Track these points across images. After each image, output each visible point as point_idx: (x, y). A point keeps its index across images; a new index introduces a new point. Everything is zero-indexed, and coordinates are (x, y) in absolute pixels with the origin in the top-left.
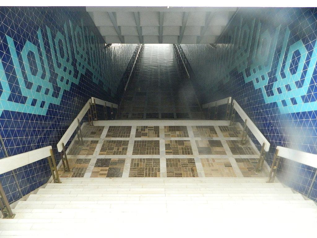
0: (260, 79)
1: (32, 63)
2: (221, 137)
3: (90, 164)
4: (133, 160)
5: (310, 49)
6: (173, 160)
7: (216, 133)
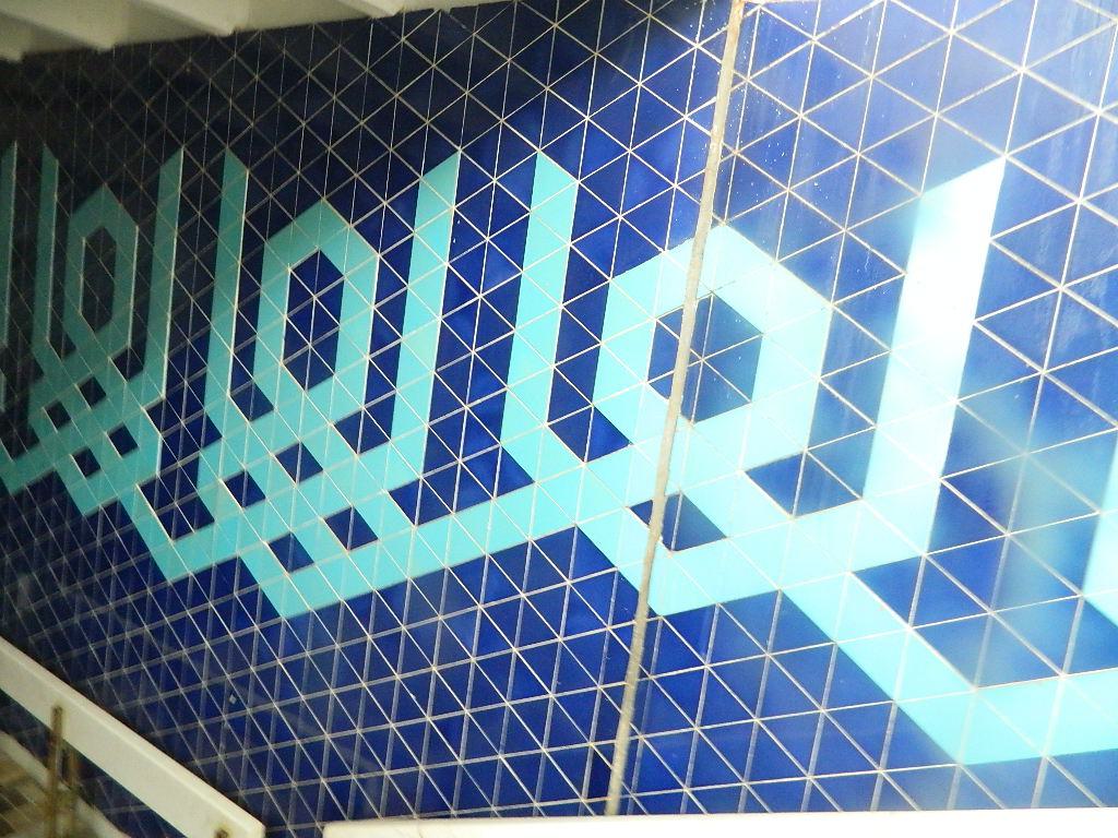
0: (107, 452)
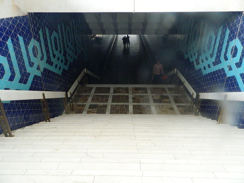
1: (56, 44)
2: (168, 94)
4: (112, 105)
7: (166, 92)
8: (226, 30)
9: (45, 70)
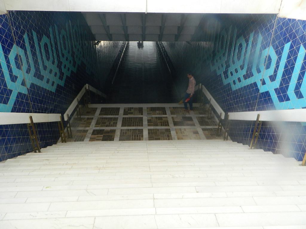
0: (221, 67)
1: (47, 52)
3: (88, 133)
4: (121, 130)
5: (247, 41)
6: (153, 130)
8: (258, 36)
9: (33, 85)
